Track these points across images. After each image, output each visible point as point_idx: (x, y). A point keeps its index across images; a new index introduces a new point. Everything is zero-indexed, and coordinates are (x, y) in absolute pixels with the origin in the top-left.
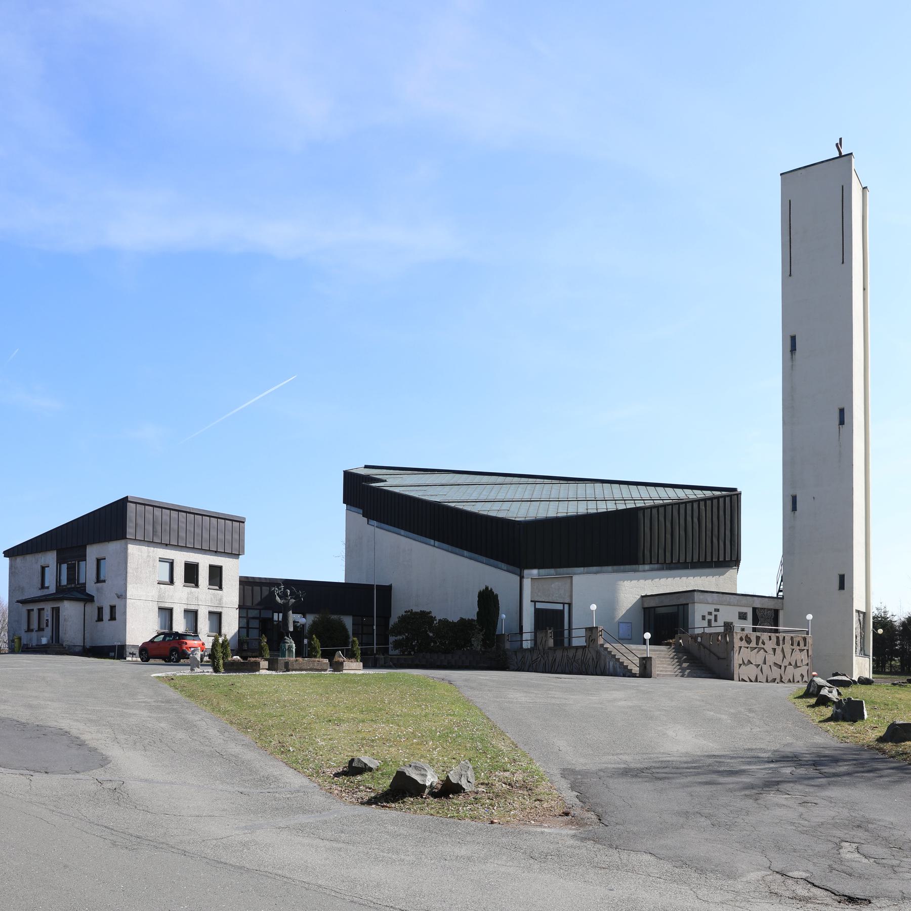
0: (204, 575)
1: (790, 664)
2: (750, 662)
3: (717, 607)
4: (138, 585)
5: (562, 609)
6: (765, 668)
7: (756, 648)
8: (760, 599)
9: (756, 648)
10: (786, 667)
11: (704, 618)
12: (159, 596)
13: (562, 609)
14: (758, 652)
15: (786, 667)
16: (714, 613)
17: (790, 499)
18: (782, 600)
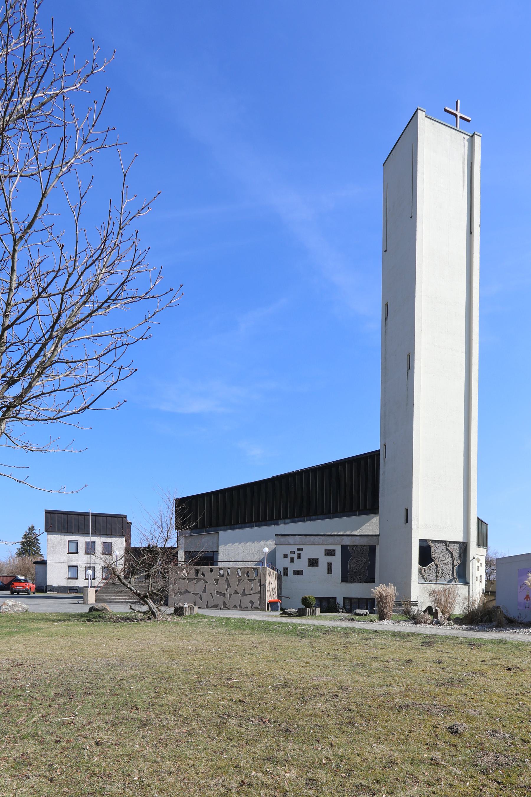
0: (99, 548)
1: (236, 592)
2: (187, 591)
3: (301, 547)
4: (54, 555)
5: (212, 555)
6: (204, 596)
7: (195, 579)
8: (350, 537)
9: (195, 579)
10: (230, 595)
11: (285, 556)
12: (68, 560)
13: (212, 555)
14: (197, 582)
15: (230, 595)
16: (297, 552)
17: (384, 306)
18: (378, 537)
